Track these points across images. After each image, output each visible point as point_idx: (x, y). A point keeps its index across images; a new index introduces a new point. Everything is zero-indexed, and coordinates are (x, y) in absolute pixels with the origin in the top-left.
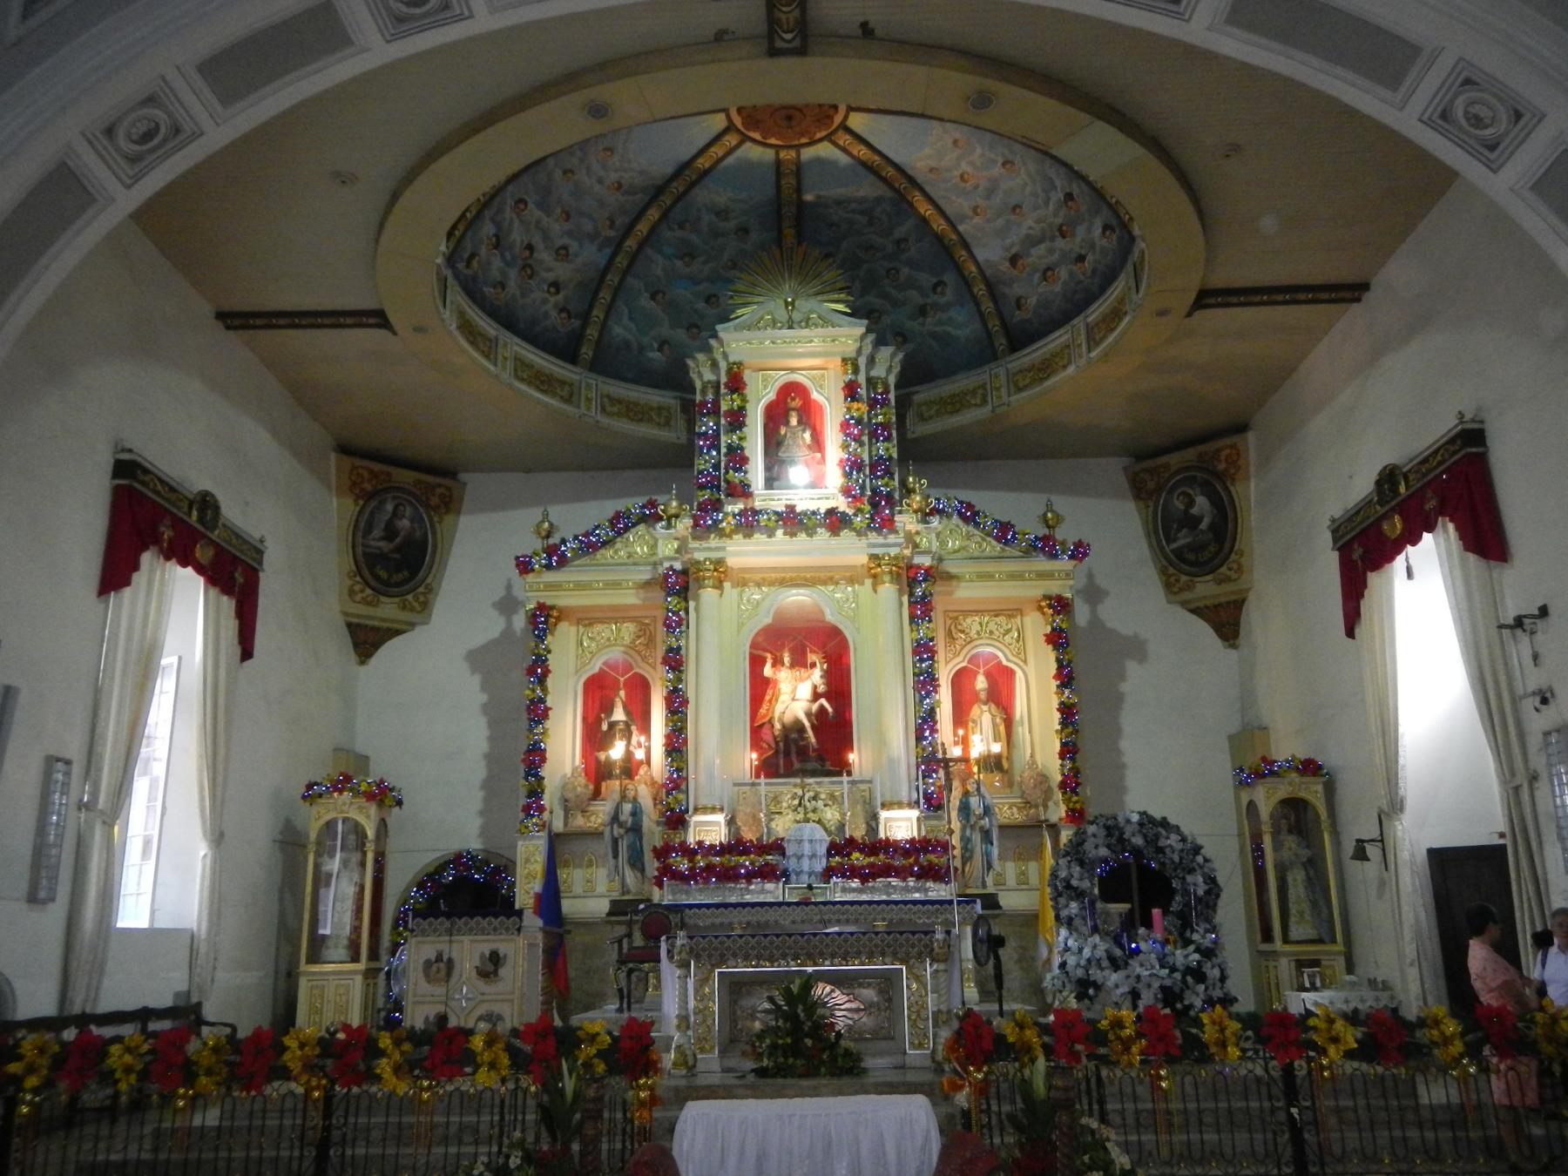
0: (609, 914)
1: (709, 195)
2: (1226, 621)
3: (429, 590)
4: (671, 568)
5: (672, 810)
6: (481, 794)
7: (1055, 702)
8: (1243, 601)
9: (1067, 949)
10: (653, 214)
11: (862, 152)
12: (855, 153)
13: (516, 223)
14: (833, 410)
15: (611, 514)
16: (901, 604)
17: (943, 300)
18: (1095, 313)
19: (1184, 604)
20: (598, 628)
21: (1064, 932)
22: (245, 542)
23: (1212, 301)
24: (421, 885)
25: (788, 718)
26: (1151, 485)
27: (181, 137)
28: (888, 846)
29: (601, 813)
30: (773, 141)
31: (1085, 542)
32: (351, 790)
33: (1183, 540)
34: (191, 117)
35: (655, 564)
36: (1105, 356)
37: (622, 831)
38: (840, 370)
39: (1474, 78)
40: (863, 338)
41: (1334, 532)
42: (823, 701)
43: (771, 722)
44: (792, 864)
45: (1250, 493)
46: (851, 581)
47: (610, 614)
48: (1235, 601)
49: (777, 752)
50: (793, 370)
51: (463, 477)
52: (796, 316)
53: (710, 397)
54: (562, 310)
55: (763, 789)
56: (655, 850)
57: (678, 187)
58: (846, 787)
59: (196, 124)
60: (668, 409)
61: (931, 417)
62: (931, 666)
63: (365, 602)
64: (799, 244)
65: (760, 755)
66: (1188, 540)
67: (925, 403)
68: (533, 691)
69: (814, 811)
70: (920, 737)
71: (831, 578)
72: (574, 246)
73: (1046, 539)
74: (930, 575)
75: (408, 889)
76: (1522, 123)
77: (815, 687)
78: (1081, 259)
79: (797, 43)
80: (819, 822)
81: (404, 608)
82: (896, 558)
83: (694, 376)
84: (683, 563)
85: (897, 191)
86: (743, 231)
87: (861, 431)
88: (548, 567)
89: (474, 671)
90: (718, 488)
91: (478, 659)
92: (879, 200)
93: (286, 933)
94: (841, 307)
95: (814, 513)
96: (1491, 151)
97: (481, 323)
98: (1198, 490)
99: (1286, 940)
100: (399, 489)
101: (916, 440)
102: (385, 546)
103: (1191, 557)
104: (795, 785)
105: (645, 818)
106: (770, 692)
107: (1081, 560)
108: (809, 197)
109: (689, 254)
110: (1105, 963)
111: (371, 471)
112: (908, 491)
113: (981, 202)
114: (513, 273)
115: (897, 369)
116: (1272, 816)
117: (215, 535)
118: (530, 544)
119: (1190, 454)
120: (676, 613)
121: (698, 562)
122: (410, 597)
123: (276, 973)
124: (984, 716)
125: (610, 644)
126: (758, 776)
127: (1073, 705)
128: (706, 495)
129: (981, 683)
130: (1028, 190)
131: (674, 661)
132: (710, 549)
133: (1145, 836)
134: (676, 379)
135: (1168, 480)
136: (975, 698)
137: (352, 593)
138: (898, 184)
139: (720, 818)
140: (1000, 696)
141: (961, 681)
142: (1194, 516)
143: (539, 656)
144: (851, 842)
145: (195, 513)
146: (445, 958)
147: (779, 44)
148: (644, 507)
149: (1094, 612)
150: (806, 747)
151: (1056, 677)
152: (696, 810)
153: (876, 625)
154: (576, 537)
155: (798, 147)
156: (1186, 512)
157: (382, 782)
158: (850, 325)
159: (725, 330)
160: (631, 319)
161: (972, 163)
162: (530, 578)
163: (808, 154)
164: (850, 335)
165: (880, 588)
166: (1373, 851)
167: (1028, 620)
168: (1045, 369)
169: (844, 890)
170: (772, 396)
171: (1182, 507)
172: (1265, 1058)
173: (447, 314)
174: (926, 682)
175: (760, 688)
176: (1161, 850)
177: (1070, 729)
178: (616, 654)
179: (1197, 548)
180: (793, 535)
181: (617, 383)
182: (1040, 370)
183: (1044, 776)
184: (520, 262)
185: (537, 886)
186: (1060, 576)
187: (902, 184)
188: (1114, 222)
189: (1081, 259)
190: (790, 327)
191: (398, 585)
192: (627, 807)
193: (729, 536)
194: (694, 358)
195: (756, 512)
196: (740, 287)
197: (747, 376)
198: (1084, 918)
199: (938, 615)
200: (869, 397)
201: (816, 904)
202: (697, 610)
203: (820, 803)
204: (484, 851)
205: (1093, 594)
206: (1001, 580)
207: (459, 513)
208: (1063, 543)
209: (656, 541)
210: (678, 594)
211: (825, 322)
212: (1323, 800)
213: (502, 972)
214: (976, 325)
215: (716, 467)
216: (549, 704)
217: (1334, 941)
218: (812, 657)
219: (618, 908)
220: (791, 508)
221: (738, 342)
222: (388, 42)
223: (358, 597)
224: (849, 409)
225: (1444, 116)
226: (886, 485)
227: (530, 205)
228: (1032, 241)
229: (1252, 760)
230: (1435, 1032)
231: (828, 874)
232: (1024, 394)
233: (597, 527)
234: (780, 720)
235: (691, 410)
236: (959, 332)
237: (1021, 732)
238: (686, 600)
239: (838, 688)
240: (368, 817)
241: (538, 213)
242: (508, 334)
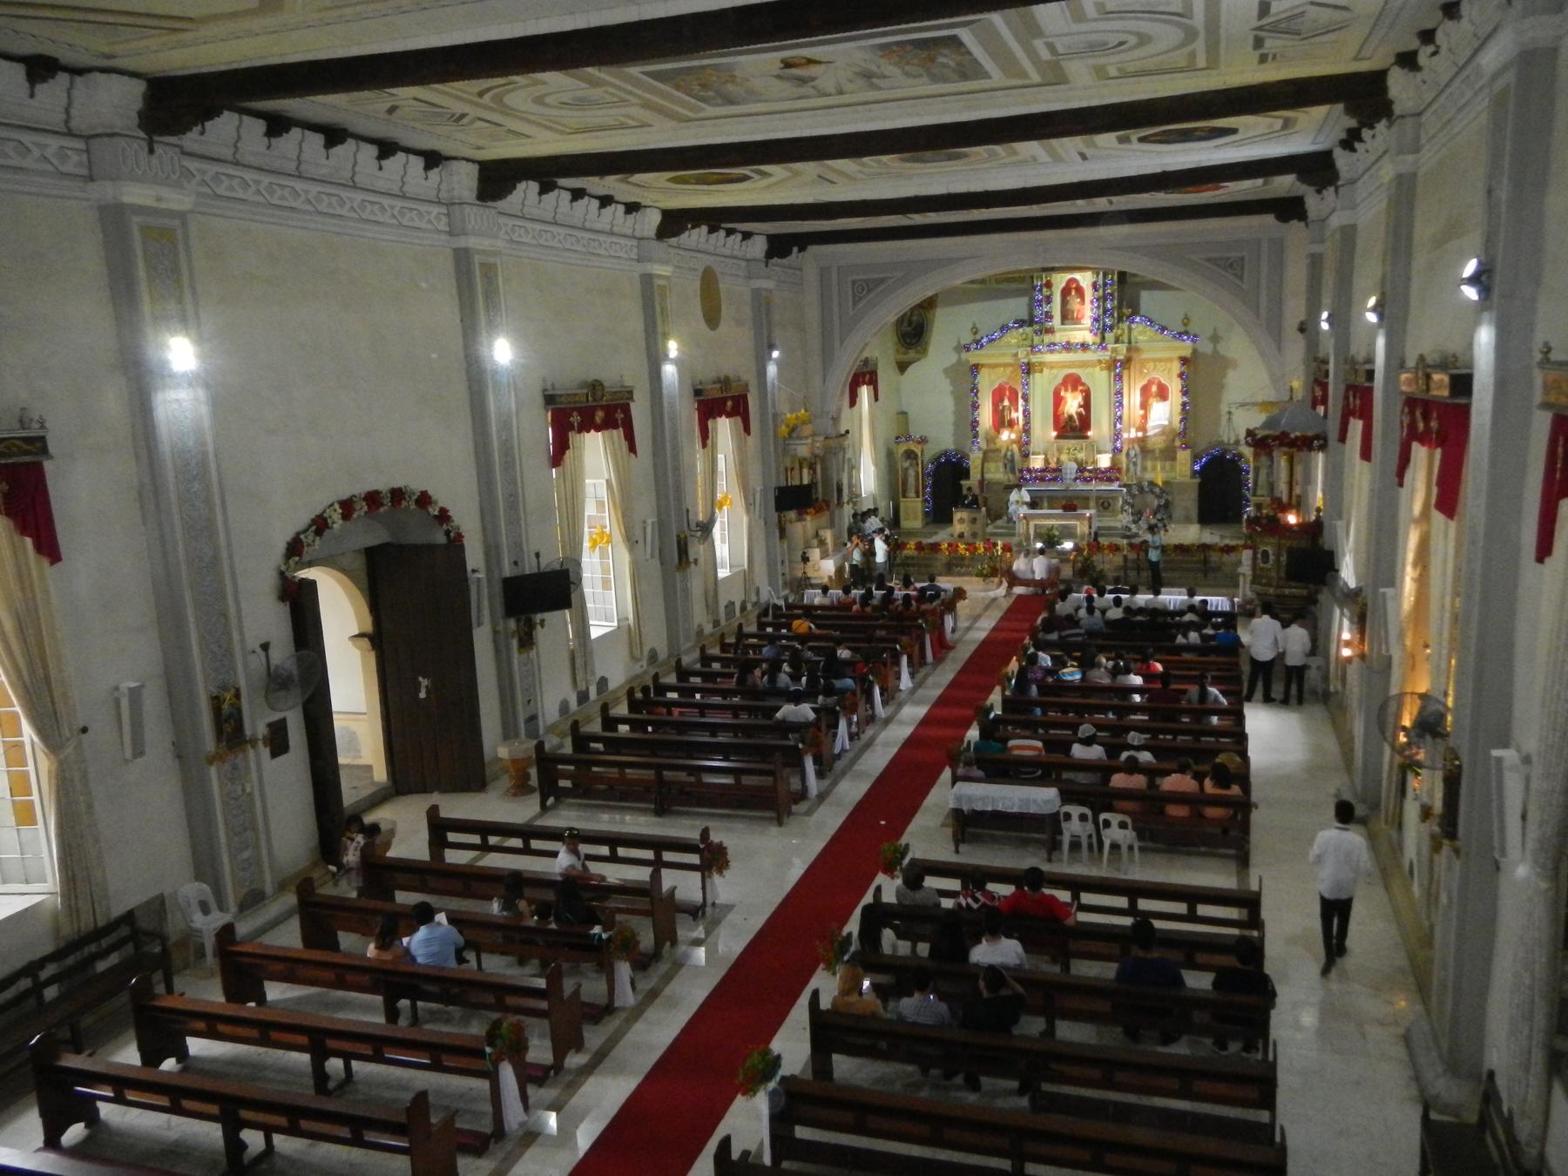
73: (1180, 334)
91: (946, 371)
118: (967, 338)
129: (1154, 388)
141: (1145, 391)
153: (1099, 381)
175: (1058, 400)
178: (1004, 379)
186: (1185, 347)
239: (1087, 404)
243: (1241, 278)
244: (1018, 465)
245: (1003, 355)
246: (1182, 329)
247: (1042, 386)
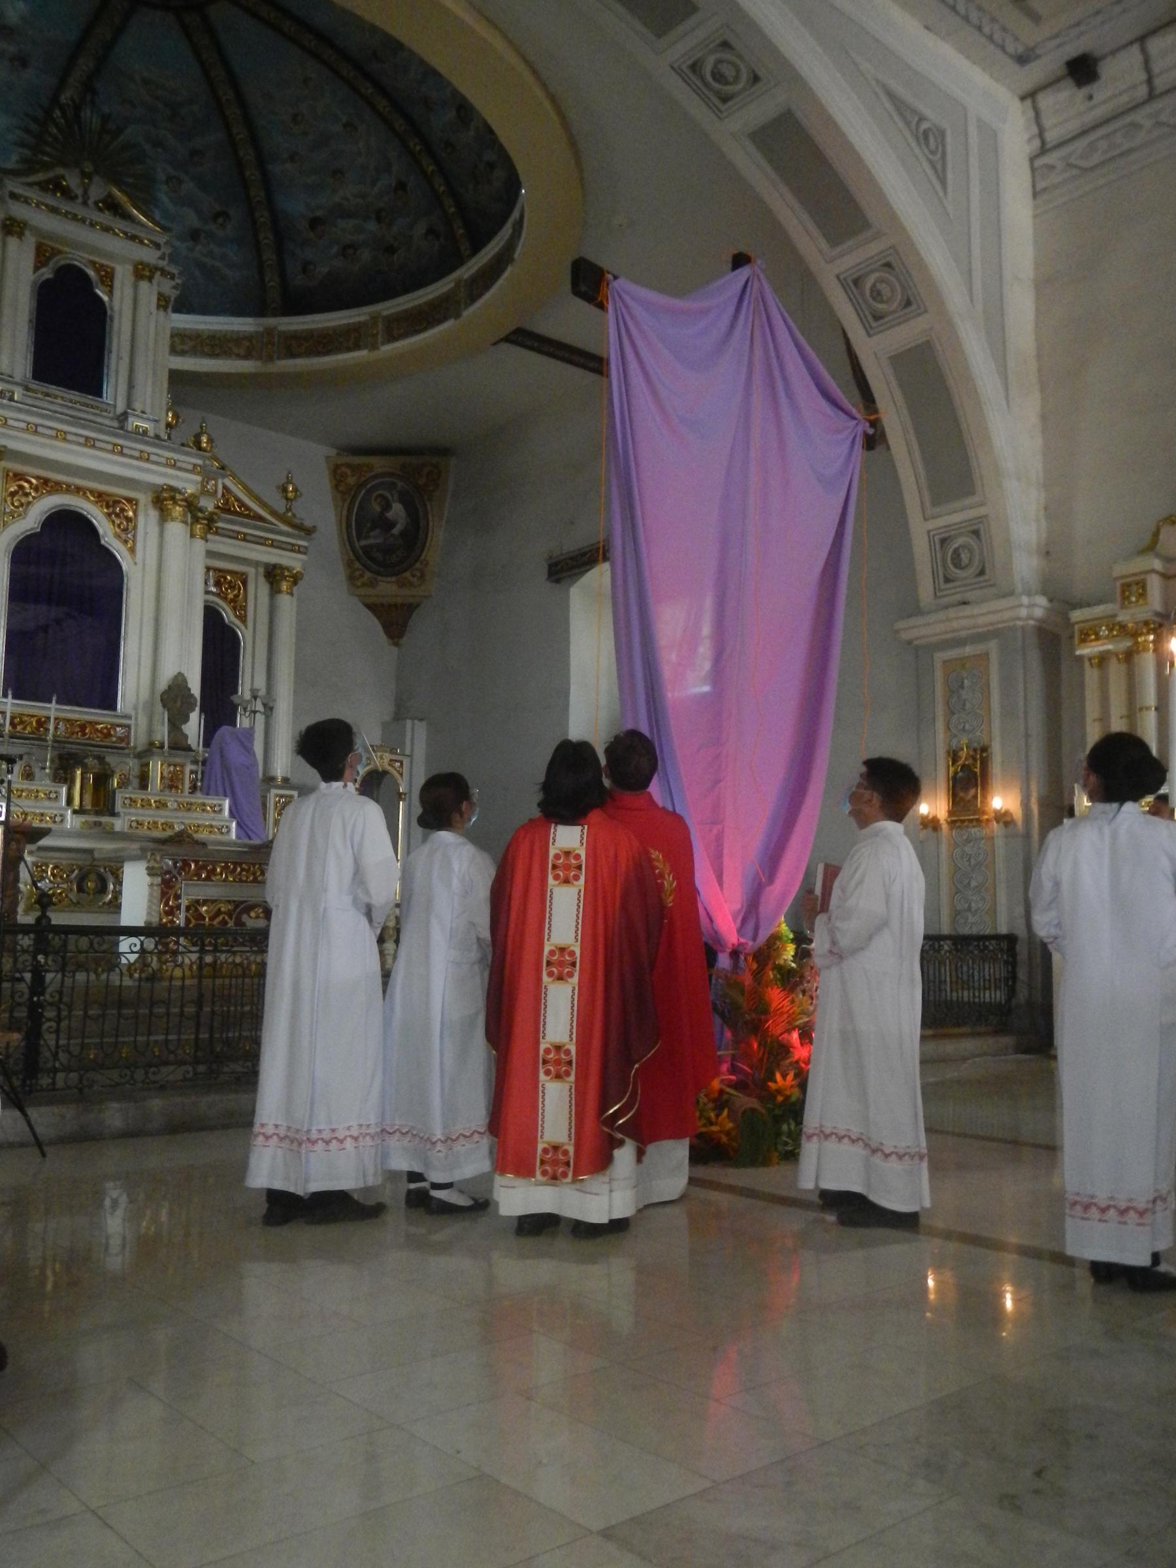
8: (418, 605)
19: (359, 596)
26: (351, 481)
33: (375, 539)
39: (894, 264)
41: (550, 566)
76: (907, 311)
78: (390, 250)
96: (875, 319)
168: (324, 343)
171: (378, 508)
189: (390, 250)
225: (856, 282)
243: (943, 182)
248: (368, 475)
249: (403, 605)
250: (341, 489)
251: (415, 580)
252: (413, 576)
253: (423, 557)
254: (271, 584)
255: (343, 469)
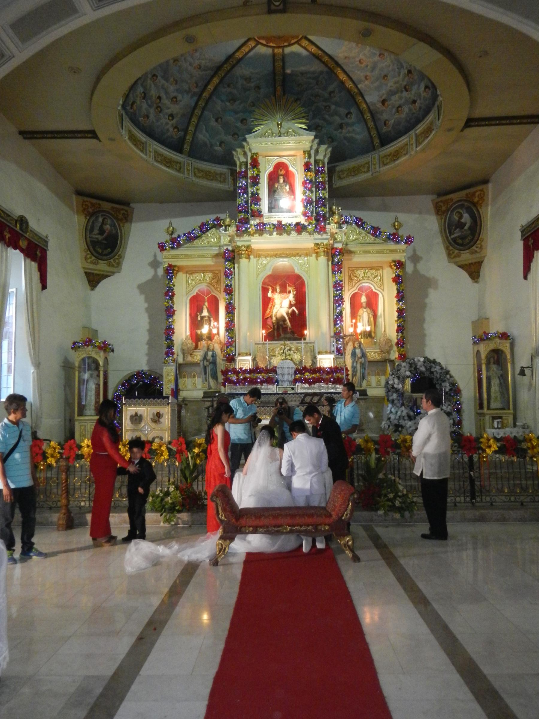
0: (203, 397)
1: (242, 71)
2: (474, 271)
3: (121, 257)
4: (227, 249)
5: (229, 355)
6: (146, 347)
7: (395, 308)
8: (482, 262)
9: (391, 412)
10: (216, 80)
11: (313, 49)
12: (310, 50)
13: (153, 86)
14: (299, 176)
15: (200, 224)
16: (328, 265)
17: (350, 121)
18: (420, 128)
19: (455, 263)
20: (195, 275)
21: (390, 405)
22: (40, 238)
23: (473, 124)
24: (123, 385)
25: (279, 315)
26: (444, 208)
27: (4, 59)
28: (320, 370)
29: (198, 356)
30: (271, 44)
31: (412, 236)
32: (92, 345)
33: (457, 233)
34: (8, 48)
35: (220, 246)
36: (423, 150)
37: (208, 363)
38: (302, 156)
40: (313, 141)
42: (294, 308)
43: (271, 317)
44: (280, 378)
45: (488, 212)
46: (307, 255)
47: (200, 269)
48: (479, 262)
49: (274, 329)
50: (281, 156)
51: (131, 205)
52: (283, 131)
53: (243, 170)
54: (176, 127)
55: (267, 346)
56: (222, 371)
57: (227, 67)
58: (303, 345)
59: (11, 52)
60: (225, 174)
61: (344, 178)
62: (341, 293)
63: (92, 263)
64: (284, 95)
65: (267, 331)
66: (460, 234)
67: (342, 171)
68: (168, 303)
69: (289, 355)
70: (335, 324)
71: (298, 254)
72: (180, 97)
73: (394, 235)
74: (341, 252)
75: (117, 386)
77: (290, 302)
78: (414, 102)
79: (281, 7)
80: (292, 360)
81: (109, 266)
82: (326, 245)
83: (236, 159)
84: (232, 247)
85: (330, 68)
86: (258, 87)
87: (312, 187)
88: (173, 248)
89: (141, 293)
90: (248, 212)
91: (142, 288)
92: (321, 73)
93: (68, 404)
94: (303, 126)
95: (290, 225)
97: (139, 135)
98: (465, 211)
99: (489, 408)
100: (104, 211)
101: (337, 188)
102: (100, 237)
103: (460, 241)
104: (281, 345)
105: (217, 358)
106: (271, 304)
107: (409, 244)
108: (288, 71)
109: (233, 99)
110: (406, 418)
111: (92, 203)
112: (332, 213)
113: (368, 74)
114: (152, 111)
115: (328, 156)
116: (487, 357)
117: (27, 235)
118: (165, 238)
119: (463, 194)
120: (229, 270)
121: (239, 247)
122: (112, 260)
123: (65, 420)
124: (364, 314)
125: (201, 282)
126: (265, 340)
127: (403, 309)
128: (242, 215)
129: (364, 299)
130: (391, 68)
131: (229, 290)
132: (244, 241)
133: (426, 367)
134: (227, 160)
135: (452, 206)
136: (361, 306)
137: (86, 258)
138: (330, 65)
139: (249, 358)
140: (372, 305)
141: (354, 298)
142: (462, 223)
143: (169, 287)
144: (305, 369)
145: (18, 226)
146: (138, 415)
147: (273, 7)
148: (214, 220)
149: (415, 267)
150: (286, 328)
151: (396, 297)
152: (239, 355)
153: (317, 274)
154: (184, 235)
155: (283, 47)
156: (459, 221)
157: (105, 342)
158: (307, 135)
159: (250, 137)
160: (207, 131)
161: (364, 55)
162: (165, 253)
163: (288, 50)
164: (307, 140)
165: (319, 258)
166: (527, 371)
167: (385, 271)
168: (396, 155)
169: (302, 388)
170: (271, 169)
171: (457, 219)
172: (462, 454)
173: (124, 132)
174: (339, 300)
175: (266, 302)
176: (432, 373)
177: (401, 320)
178: (203, 287)
179: (463, 238)
180: (281, 234)
181: (203, 162)
182: (394, 156)
183: (389, 340)
184: (155, 106)
185: (172, 386)
186: (400, 251)
187: (332, 64)
188: (430, 85)
189: (414, 102)
190: (280, 136)
191: (106, 255)
192: (210, 353)
193: (253, 235)
194: (235, 150)
195: (264, 224)
196: (257, 117)
197: (260, 159)
198: (399, 400)
199: (345, 270)
200: (316, 170)
201: (290, 394)
202: (239, 268)
203: (292, 352)
204: (149, 370)
205: (415, 258)
206: (373, 253)
207: (131, 222)
208: (402, 237)
209: (220, 238)
210: (230, 261)
211: (296, 133)
212: (509, 350)
213: (161, 420)
214: (366, 133)
215: (247, 202)
216: (175, 308)
217: (509, 409)
218: (289, 289)
219: (207, 395)
220: (280, 222)
221: (255, 143)
222: (94, 10)
223: (89, 261)
224: (306, 175)
226: (323, 211)
227: (159, 78)
228: (392, 93)
229: (481, 332)
230: (529, 444)
231: (295, 381)
232: (387, 167)
233: (194, 230)
234: (275, 316)
235: (235, 175)
236: (358, 137)
237: (381, 320)
238: (234, 263)
239: (300, 301)
240: (100, 356)
241: (163, 82)
242: (151, 140)
244: (221, 365)
245: (202, 256)
246: (393, 231)
247: (249, 275)
248: (451, 204)
249: (475, 263)
250: (440, 213)
251: (477, 249)
252: (477, 247)
253: (480, 238)
254: (392, 268)
255: (440, 204)
